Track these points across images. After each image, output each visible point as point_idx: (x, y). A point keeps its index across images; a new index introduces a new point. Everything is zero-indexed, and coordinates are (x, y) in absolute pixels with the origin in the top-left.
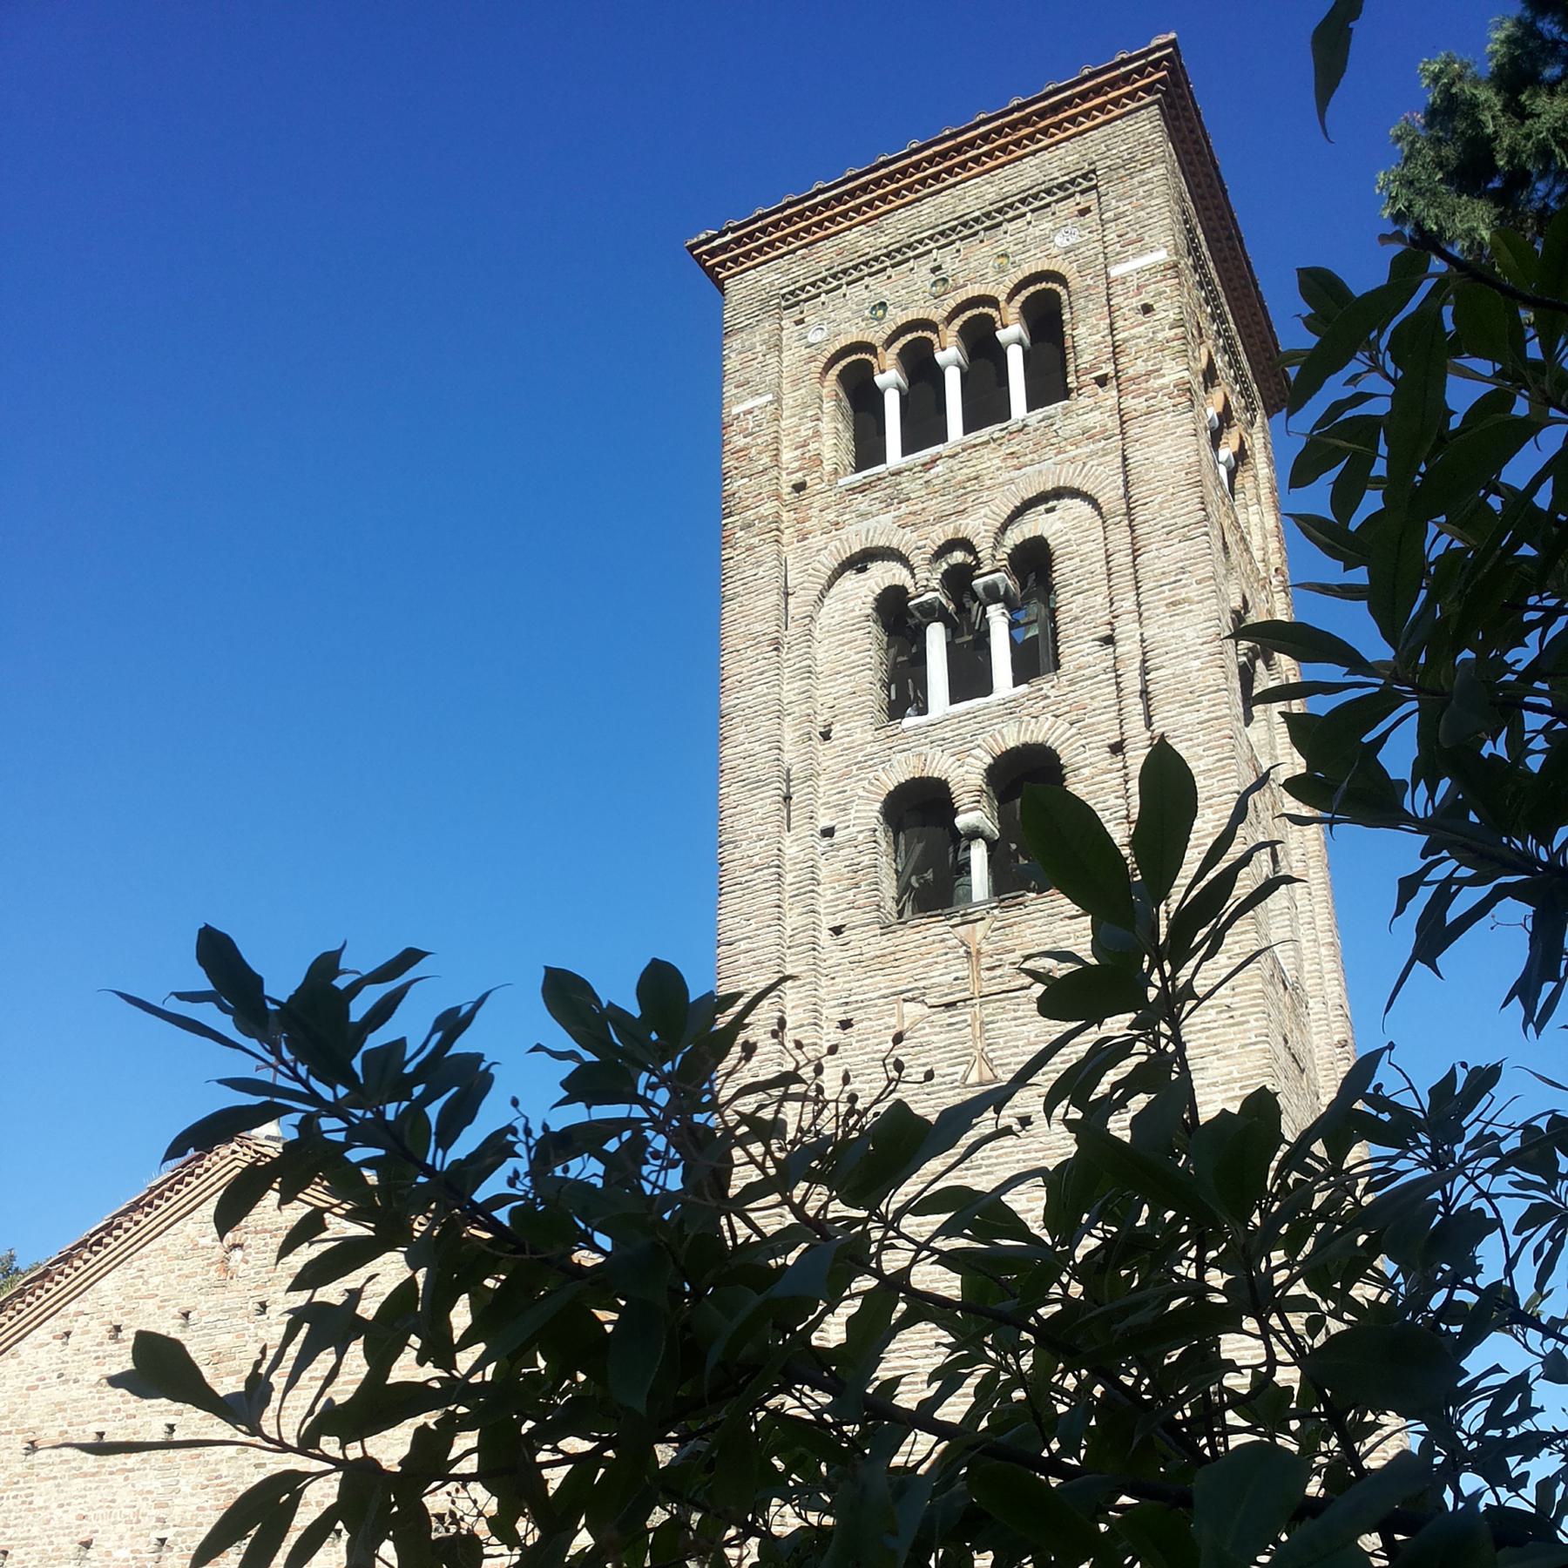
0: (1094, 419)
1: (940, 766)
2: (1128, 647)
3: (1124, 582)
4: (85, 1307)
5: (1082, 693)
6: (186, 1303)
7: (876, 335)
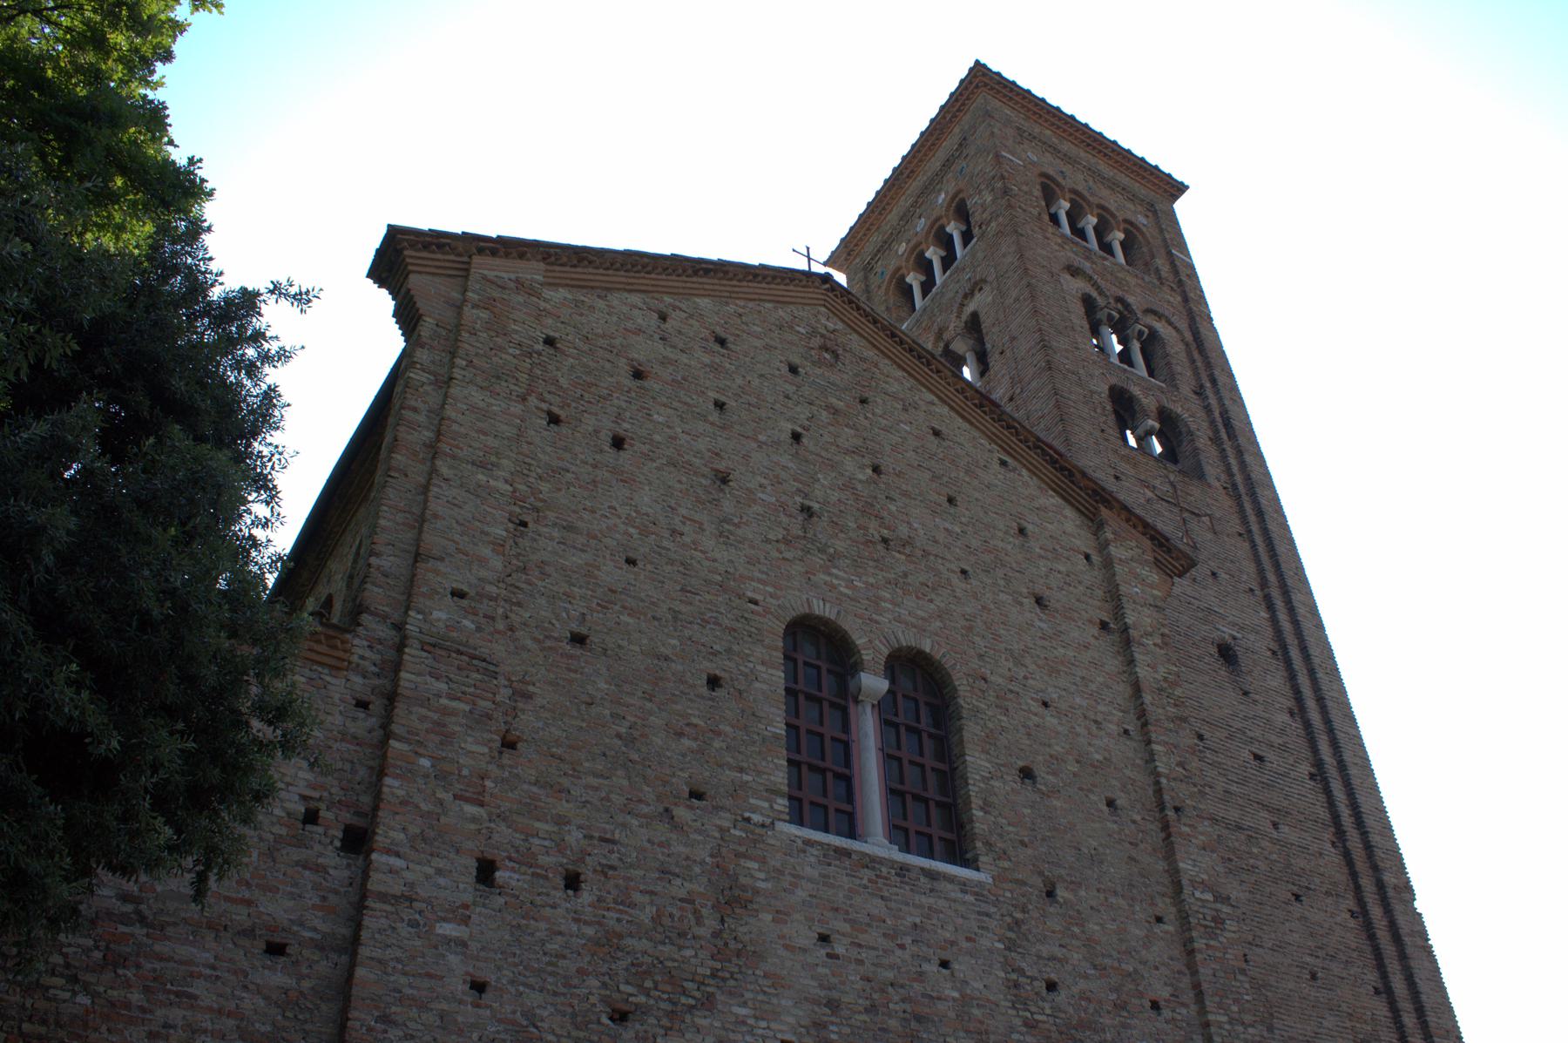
4: (683, 306)
6: (796, 360)
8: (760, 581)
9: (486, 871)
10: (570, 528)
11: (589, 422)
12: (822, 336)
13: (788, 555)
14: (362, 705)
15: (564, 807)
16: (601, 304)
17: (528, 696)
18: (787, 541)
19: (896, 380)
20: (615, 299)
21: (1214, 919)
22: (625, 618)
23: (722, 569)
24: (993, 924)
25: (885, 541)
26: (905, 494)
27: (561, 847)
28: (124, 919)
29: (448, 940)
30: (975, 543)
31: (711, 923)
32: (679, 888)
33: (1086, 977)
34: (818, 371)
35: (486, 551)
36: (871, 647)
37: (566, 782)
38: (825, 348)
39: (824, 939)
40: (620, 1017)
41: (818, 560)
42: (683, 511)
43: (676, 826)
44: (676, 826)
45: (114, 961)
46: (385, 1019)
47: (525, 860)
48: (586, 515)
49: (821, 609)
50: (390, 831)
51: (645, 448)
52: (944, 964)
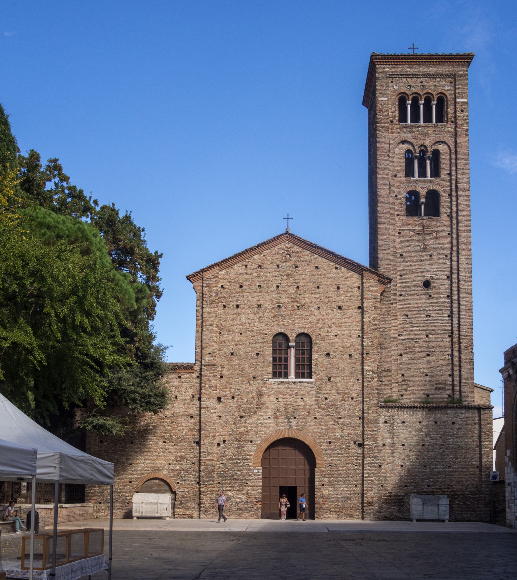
0: (450, 129)
1: (418, 189)
2: (454, 177)
3: (453, 165)
5: (444, 183)
6: (278, 263)
7: (409, 92)
8: (268, 329)
9: (219, 399)
10: (229, 331)
11: (231, 304)
12: (287, 251)
13: (274, 320)
14: (198, 377)
15: (231, 386)
16: (232, 270)
17: (224, 368)
18: (274, 317)
19: (307, 255)
20: (235, 267)
21: (371, 378)
22: (240, 347)
23: (259, 329)
24: (314, 389)
25: (298, 307)
26: (305, 292)
27: (231, 392)
28: (172, 417)
29: (213, 412)
30: (323, 298)
31: (256, 400)
32: (251, 395)
33: (335, 396)
34: (284, 264)
35: (213, 343)
36: (292, 336)
37: (231, 381)
38: (287, 254)
39: (277, 399)
40: (241, 417)
41: (281, 319)
42: (251, 318)
43: (250, 384)
44: (250, 384)
45: (173, 422)
46: (206, 425)
47: (225, 396)
48: (232, 327)
49: (281, 330)
50: (204, 398)
51: (243, 306)
52: (302, 399)
